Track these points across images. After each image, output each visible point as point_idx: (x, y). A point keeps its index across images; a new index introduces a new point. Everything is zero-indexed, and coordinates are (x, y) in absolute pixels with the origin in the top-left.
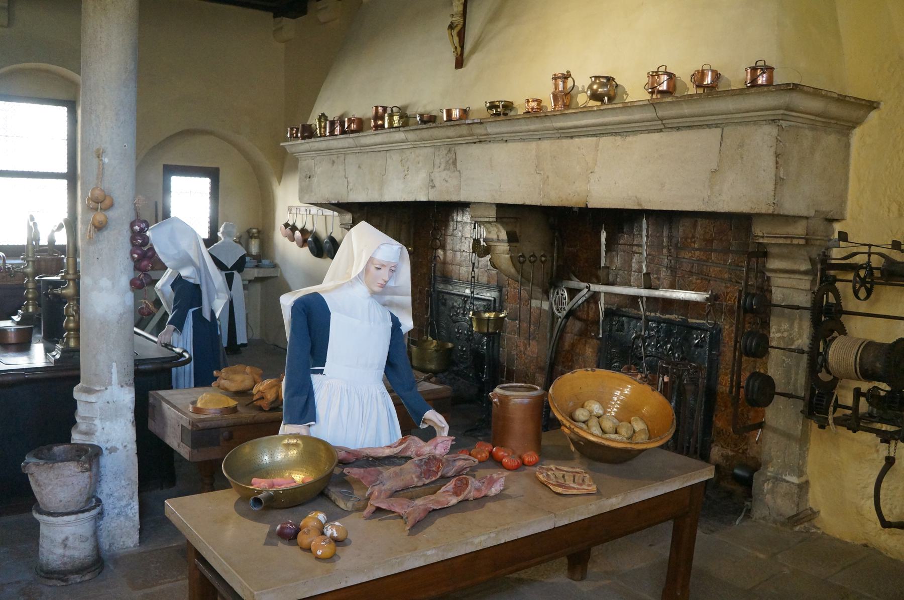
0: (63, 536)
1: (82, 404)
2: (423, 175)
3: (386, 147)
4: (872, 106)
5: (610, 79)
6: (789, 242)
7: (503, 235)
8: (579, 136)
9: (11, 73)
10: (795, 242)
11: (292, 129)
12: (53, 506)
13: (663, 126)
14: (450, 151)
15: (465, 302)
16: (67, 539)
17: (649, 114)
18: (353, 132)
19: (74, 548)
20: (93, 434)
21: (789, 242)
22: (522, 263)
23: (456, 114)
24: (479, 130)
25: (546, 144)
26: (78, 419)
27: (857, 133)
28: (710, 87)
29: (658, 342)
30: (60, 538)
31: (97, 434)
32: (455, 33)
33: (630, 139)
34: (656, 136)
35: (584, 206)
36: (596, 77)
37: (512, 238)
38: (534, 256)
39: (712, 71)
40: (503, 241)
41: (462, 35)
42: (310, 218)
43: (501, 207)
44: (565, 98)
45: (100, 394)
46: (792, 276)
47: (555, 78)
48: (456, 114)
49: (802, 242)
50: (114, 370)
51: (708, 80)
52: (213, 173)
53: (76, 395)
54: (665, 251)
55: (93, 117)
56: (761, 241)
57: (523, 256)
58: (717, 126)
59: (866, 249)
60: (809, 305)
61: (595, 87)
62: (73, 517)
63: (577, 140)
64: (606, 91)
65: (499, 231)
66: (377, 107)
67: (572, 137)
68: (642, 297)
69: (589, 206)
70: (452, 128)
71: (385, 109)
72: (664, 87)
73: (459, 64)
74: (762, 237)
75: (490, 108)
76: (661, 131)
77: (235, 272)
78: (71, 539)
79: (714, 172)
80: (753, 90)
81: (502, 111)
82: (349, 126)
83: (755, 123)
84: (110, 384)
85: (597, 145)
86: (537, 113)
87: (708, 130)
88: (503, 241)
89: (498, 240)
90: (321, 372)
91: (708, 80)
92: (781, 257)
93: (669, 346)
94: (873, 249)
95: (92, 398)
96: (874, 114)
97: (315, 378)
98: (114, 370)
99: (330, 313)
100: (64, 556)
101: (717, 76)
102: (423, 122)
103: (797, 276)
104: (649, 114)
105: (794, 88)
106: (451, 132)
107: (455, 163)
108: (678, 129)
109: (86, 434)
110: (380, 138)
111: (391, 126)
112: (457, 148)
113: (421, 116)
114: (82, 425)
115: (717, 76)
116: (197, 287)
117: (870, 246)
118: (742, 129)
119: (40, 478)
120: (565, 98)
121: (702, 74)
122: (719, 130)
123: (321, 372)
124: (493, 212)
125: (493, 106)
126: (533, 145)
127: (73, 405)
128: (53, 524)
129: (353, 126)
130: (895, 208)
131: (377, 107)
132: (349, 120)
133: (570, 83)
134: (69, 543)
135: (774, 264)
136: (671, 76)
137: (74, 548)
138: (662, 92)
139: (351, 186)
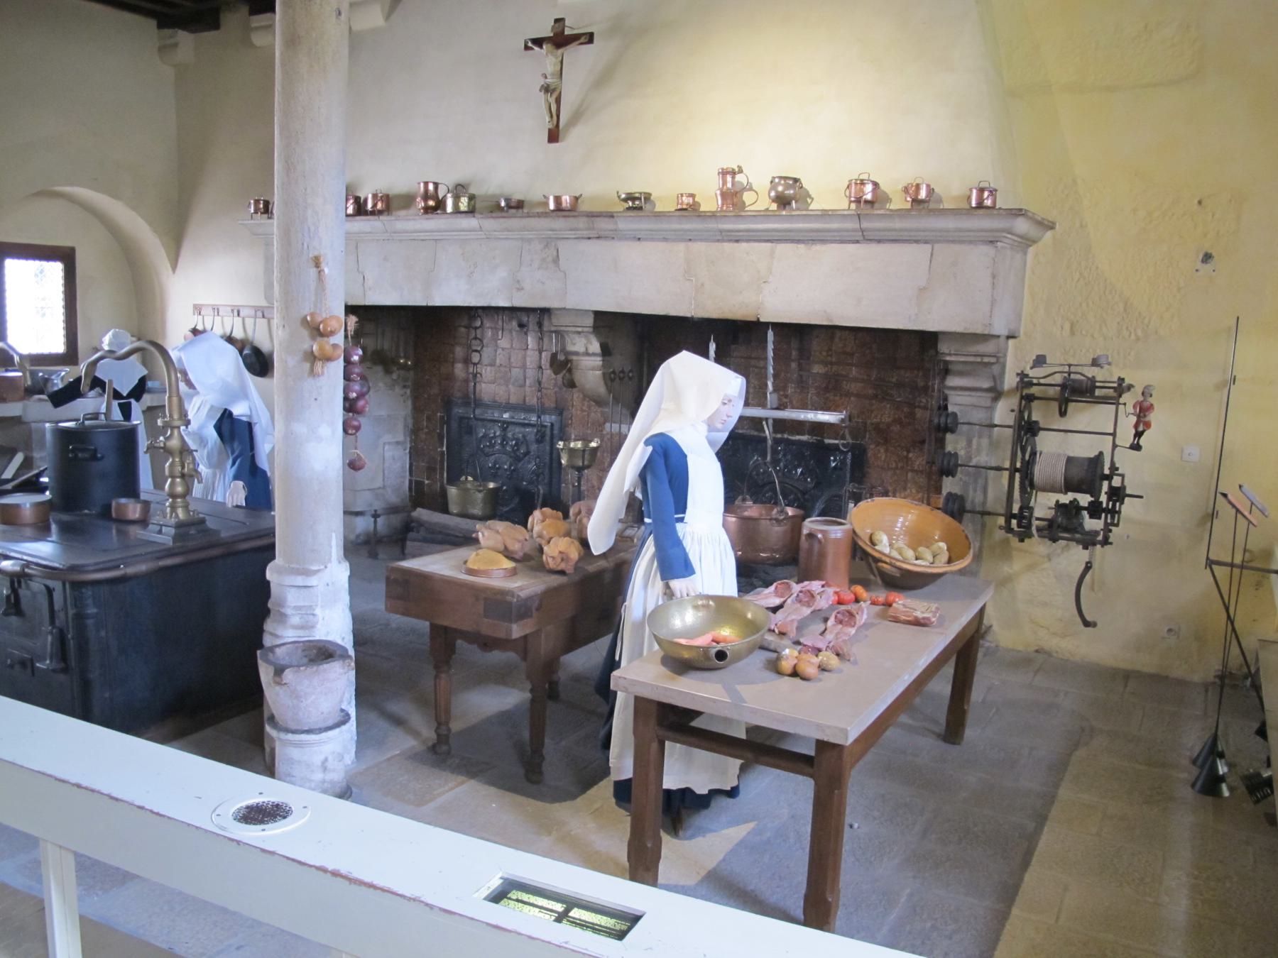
0: (322, 757)
1: (293, 590)
2: (502, 273)
3: (437, 236)
4: (1051, 226)
5: (796, 180)
6: (979, 359)
7: (595, 347)
8: (748, 241)
9: (289, 167)
10: (986, 360)
11: (257, 202)
12: (314, 719)
13: (865, 237)
14: (547, 246)
15: (504, 430)
16: (326, 760)
17: (852, 225)
18: (380, 212)
19: (334, 770)
20: (313, 627)
21: (979, 359)
22: (612, 380)
23: (566, 200)
24: (603, 224)
25: (699, 247)
26: (289, 611)
27: (1031, 250)
28: (921, 204)
29: (785, 467)
30: (317, 760)
31: (319, 626)
32: (552, 100)
33: (818, 248)
34: (851, 247)
35: (754, 319)
36: (781, 178)
37: (606, 351)
38: (622, 372)
39: (928, 186)
40: (594, 354)
41: (558, 101)
42: (238, 321)
43: (599, 316)
44: (732, 197)
45: (320, 575)
46: (973, 394)
47: (724, 173)
48: (566, 200)
49: (993, 360)
50: (334, 543)
51: (923, 194)
52: (66, 257)
53: (268, 576)
54: (794, 365)
55: (309, 212)
56: (948, 358)
57: (614, 372)
58: (926, 242)
59: (1066, 369)
60: (1012, 423)
61: (780, 189)
62: (337, 731)
63: (744, 245)
64: (789, 196)
65: (589, 342)
66: (426, 184)
67: (737, 241)
68: (767, 419)
69: (762, 320)
70: (562, 220)
71: (436, 185)
72: (869, 197)
73: (553, 136)
74: (950, 355)
75: (625, 200)
76: (857, 242)
77: (133, 401)
78: (330, 758)
79: (922, 290)
80: (981, 212)
81: (637, 203)
82: (375, 205)
83: (971, 242)
84: (330, 561)
85: (772, 254)
86: (690, 210)
87: (914, 245)
88: (594, 354)
89: (587, 354)
90: (682, 520)
91: (923, 194)
92: (961, 374)
93: (799, 470)
94: (1073, 369)
95: (313, 581)
96: (1049, 234)
97: (679, 526)
98: (334, 543)
99: (685, 456)
100: (324, 781)
101: (930, 191)
102: (509, 206)
103: (979, 394)
104: (852, 225)
105: (1019, 213)
106: (559, 223)
107: (556, 260)
108: (879, 241)
109: (302, 627)
110: (434, 222)
111: (457, 211)
112: (561, 244)
113: (507, 200)
114: (295, 620)
115: (930, 191)
116: (250, 426)
117: (1070, 365)
118: (956, 247)
119: (299, 688)
120: (732, 197)
121: (918, 187)
122: (928, 247)
123: (682, 520)
124: (589, 321)
125: (630, 197)
126: (681, 246)
127: (264, 588)
128: (310, 744)
129: (379, 206)
130: (1067, 326)
131: (426, 184)
132: (375, 196)
133: (739, 178)
134: (330, 765)
135: (952, 381)
136: (876, 184)
137: (334, 770)
138: (866, 202)
139: (369, 283)
